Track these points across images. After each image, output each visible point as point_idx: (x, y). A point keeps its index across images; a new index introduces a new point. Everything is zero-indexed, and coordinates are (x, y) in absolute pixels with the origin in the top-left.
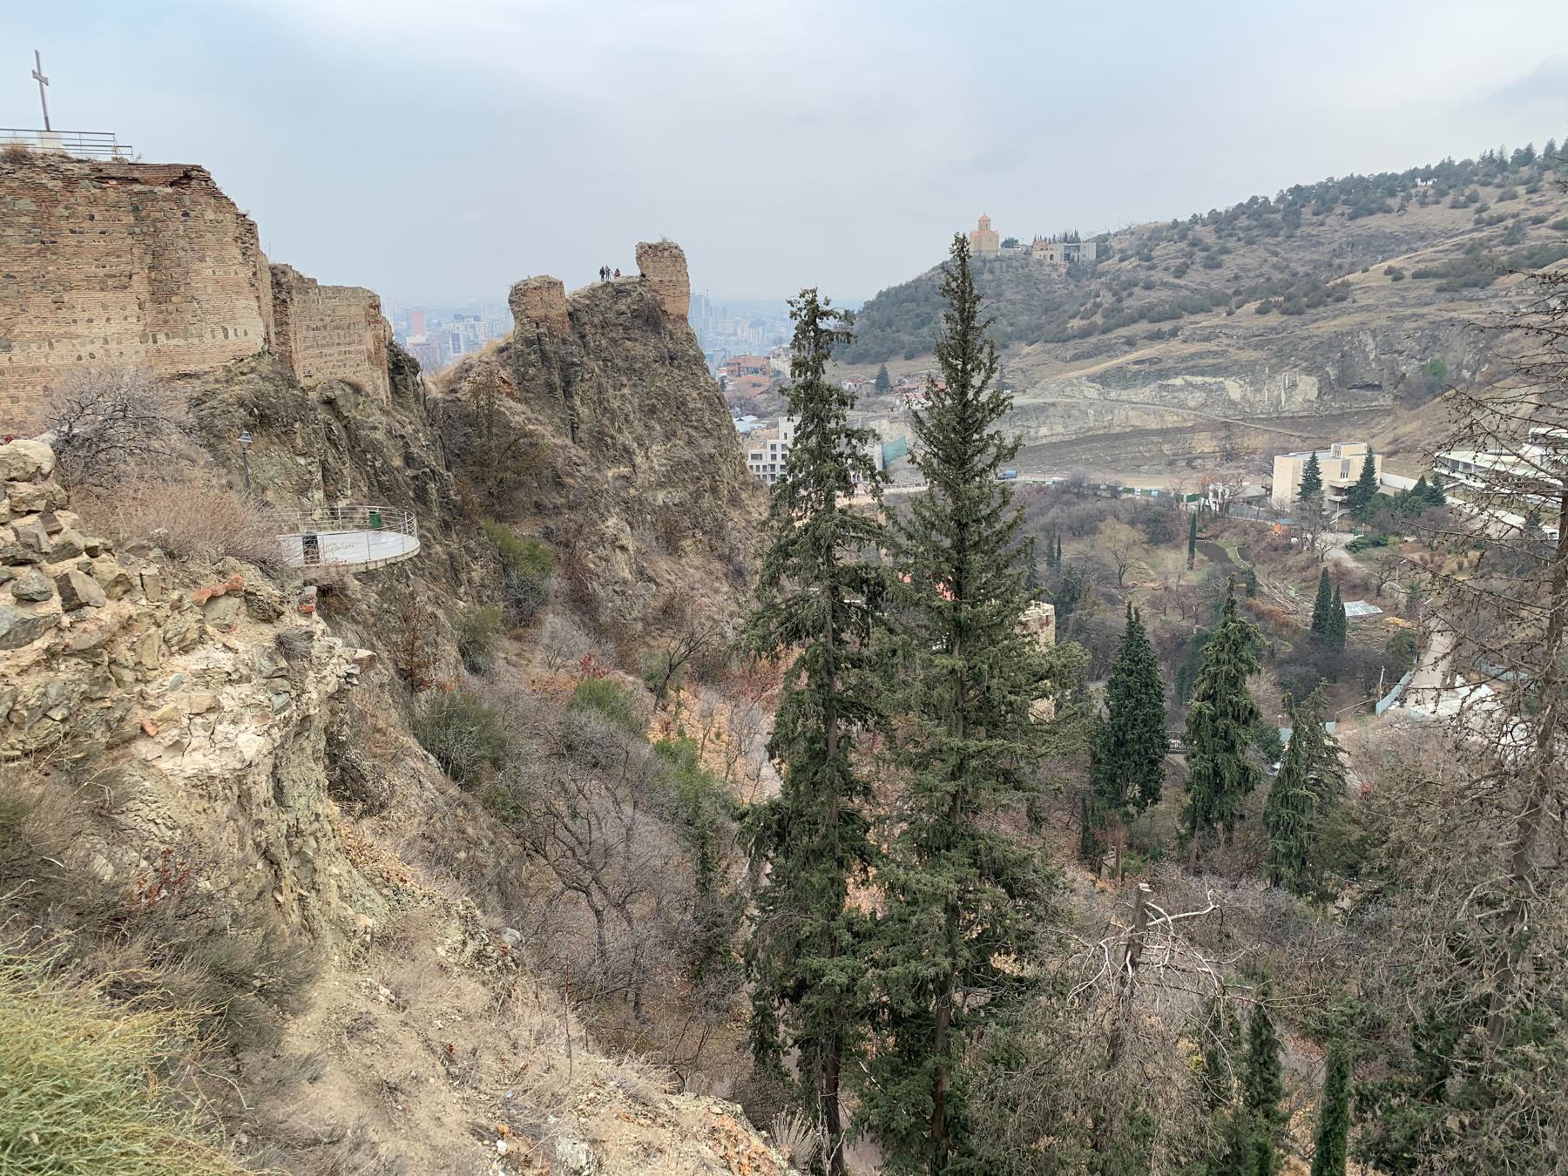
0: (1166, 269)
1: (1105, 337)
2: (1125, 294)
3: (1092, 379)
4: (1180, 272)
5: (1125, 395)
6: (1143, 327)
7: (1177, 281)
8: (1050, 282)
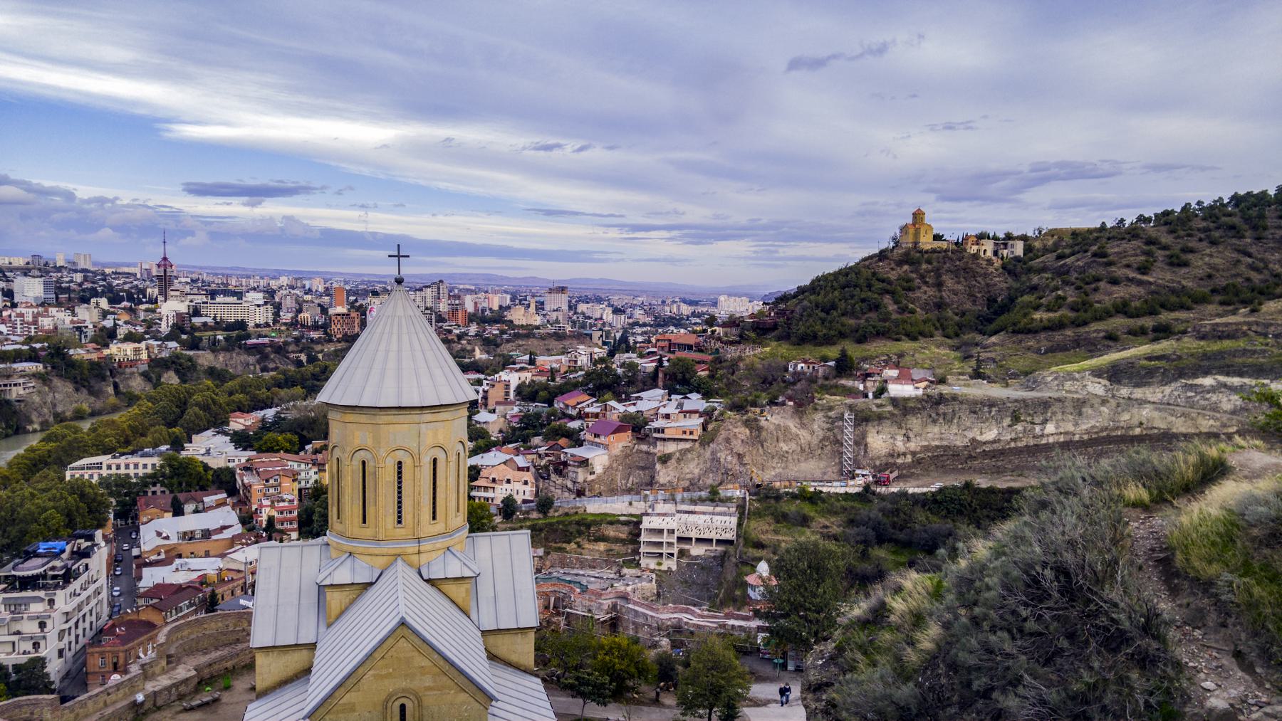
0: (1128, 266)
1: (1082, 330)
2: (1088, 288)
3: (1097, 373)
4: (1144, 269)
5: (1138, 393)
6: (1119, 322)
7: (1145, 278)
8: (986, 275)
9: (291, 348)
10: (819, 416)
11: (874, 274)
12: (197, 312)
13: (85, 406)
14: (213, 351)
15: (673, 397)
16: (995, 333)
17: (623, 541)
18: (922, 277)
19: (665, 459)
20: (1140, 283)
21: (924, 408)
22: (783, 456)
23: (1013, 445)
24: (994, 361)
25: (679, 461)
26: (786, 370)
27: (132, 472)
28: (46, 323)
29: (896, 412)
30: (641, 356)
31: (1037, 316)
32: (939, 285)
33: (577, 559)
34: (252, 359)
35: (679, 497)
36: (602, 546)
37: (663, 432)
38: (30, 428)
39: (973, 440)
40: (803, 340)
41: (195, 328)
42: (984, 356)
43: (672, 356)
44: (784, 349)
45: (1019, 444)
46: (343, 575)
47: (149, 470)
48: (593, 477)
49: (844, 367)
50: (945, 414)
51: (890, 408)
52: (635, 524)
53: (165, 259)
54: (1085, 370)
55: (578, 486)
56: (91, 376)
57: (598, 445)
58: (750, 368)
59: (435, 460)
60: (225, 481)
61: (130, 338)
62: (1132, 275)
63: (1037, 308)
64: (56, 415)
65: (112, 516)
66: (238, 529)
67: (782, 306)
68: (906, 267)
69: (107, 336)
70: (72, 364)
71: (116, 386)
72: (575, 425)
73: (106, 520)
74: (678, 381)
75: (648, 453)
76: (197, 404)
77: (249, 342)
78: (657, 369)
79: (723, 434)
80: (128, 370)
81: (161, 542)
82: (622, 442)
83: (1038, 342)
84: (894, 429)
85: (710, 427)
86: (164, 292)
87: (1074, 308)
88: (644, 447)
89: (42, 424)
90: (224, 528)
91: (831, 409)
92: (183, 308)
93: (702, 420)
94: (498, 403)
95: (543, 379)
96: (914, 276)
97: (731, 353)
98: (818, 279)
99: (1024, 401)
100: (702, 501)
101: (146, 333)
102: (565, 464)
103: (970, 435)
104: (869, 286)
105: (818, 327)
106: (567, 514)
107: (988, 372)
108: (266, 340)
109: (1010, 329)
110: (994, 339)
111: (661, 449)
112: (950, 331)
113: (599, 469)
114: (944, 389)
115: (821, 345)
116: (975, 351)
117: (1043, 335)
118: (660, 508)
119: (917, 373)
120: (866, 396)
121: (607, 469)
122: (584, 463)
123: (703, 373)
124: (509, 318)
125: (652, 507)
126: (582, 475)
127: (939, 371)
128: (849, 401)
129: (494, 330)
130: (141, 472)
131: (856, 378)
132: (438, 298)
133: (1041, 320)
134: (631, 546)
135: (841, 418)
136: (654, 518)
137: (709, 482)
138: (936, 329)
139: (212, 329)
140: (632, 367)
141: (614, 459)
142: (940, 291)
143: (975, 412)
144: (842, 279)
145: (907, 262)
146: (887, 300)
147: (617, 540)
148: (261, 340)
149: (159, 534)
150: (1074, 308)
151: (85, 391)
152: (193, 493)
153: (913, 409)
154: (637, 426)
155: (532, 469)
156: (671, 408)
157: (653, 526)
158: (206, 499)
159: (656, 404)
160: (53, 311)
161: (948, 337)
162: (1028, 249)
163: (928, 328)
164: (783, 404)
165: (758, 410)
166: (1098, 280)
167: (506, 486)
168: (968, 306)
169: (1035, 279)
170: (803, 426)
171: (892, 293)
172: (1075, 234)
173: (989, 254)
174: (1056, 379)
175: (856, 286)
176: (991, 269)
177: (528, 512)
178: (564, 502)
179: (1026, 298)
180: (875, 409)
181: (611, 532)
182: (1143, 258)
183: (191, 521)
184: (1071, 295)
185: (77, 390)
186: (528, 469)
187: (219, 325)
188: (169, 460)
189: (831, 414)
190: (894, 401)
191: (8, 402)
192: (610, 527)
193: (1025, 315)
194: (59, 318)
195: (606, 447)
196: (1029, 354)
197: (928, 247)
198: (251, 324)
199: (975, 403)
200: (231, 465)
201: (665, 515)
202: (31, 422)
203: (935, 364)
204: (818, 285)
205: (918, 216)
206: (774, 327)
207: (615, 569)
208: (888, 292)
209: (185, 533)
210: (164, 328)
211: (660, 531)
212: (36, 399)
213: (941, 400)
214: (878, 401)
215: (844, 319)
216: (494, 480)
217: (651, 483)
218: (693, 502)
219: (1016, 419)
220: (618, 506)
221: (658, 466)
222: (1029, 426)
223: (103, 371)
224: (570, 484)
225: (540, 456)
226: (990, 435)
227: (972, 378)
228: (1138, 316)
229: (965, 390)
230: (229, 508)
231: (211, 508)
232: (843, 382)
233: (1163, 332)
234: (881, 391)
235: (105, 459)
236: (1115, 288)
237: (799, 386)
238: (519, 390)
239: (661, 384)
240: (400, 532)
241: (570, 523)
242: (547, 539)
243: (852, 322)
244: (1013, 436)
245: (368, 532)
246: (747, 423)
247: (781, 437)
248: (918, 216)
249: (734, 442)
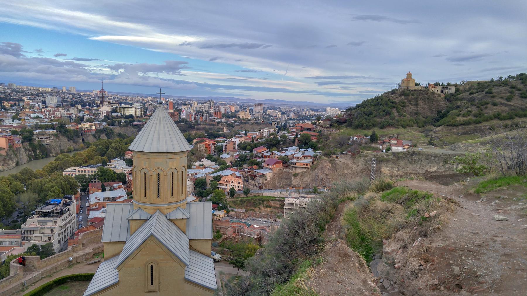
0: (502, 98)
1: (478, 125)
2: (482, 107)
4: (509, 99)
6: (496, 122)
7: (509, 103)
8: (437, 101)
10: (361, 159)
11: (389, 100)
12: (114, 111)
13: (72, 147)
15: (301, 150)
16: (440, 126)
17: (277, 208)
18: (410, 101)
19: (296, 175)
20: (506, 105)
21: (406, 157)
22: (345, 176)
23: (444, 173)
24: (438, 138)
25: (301, 176)
26: (349, 139)
27: (87, 173)
28: (58, 114)
29: (394, 158)
30: (289, 133)
31: (458, 119)
32: (417, 105)
33: (258, 214)
35: (301, 191)
36: (269, 209)
37: (295, 164)
38: (51, 155)
39: (427, 171)
41: (113, 118)
42: (434, 135)
43: (302, 133)
44: (349, 130)
45: (446, 173)
46: (137, 217)
47: (93, 173)
48: (266, 181)
49: (374, 139)
50: (415, 160)
51: (392, 157)
52: (282, 201)
53: (102, 89)
54: (478, 143)
55: (260, 185)
56: (75, 135)
57: (269, 169)
59: (173, 173)
60: (122, 179)
61: (89, 121)
62: (503, 101)
63: (458, 115)
64: (61, 150)
65: (79, 190)
66: (126, 197)
67: (349, 113)
68: (403, 97)
69: (81, 120)
70: (67, 131)
71: (83, 140)
72: (260, 160)
73: (77, 192)
74: (304, 143)
75: (289, 173)
76: (112, 148)
77: (134, 123)
78: (295, 139)
79: (320, 166)
80: (87, 133)
81: (96, 201)
82: (280, 166)
83: (458, 130)
84: (393, 165)
85: (315, 163)
86: (102, 102)
87: (475, 116)
88: (287, 170)
89: (56, 154)
90: (121, 197)
91: (367, 156)
92: (109, 109)
93: (312, 160)
94: (230, 151)
95: (249, 141)
96: (406, 101)
97: (326, 132)
98: (365, 101)
99: (449, 155)
100: (310, 193)
101: (95, 119)
102: (255, 176)
103: (426, 169)
104: (387, 105)
105: (364, 122)
106: (255, 196)
107: (435, 142)
109: (446, 125)
110: (439, 128)
111: (294, 171)
112: (420, 125)
113: (268, 178)
114: (415, 149)
115: (365, 129)
116: (430, 133)
117: (460, 127)
118: (293, 195)
119: (405, 142)
120: (382, 151)
121: (272, 179)
122: (263, 176)
124: (238, 116)
125: (290, 194)
126: (261, 181)
127: (415, 142)
128: (374, 153)
129: (232, 121)
130: (90, 173)
131: (379, 143)
132: (210, 107)
133: (460, 121)
134: (280, 210)
135: (371, 160)
136: (290, 199)
137: (314, 185)
138: (415, 123)
139: (120, 118)
140: (285, 137)
141: (275, 174)
142: (417, 107)
143: (428, 159)
144: (375, 102)
145: (403, 95)
146: (394, 111)
147: (275, 207)
148: (139, 123)
149: (96, 198)
150: (475, 116)
151: (72, 141)
152: (110, 183)
154: (285, 161)
155: (242, 177)
156: (299, 155)
157: (289, 202)
158: (114, 185)
159: (293, 153)
160: (60, 109)
161: (419, 127)
162: (457, 90)
163: (411, 123)
164: (346, 154)
165: (335, 156)
166: (487, 104)
167: (231, 184)
168: (429, 114)
169: (459, 103)
170: (354, 163)
171: (396, 108)
172: (479, 83)
173: (439, 92)
174: (464, 146)
175: (381, 105)
176: (440, 99)
177: (240, 195)
178: (254, 191)
179: (454, 111)
180: (385, 157)
181: (272, 204)
182: (509, 94)
183: (108, 194)
184: (474, 110)
185: (69, 141)
186: (240, 177)
187: (122, 116)
188: (101, 170)
189: (367, 158)
190: (394, 154)
191: (43, 145)
192: (272, 202)
193: (453, 119)
194: (62, 112)
195: (272, 169)
197: (413, 89)
198: (135, 116)
199: (428, 155)
200: (125, 172)
201: (294, 198)
202: (52, 153)
203: (413, 139)
204: (364, 104)
205: (409, 75)
206: (345, 122)
207: (273, 219)
208: (394, 107)
209: (106, 198)
210: (102, 117)
211: (293, 204)
212: (54, 144)
213: (414, 154)
214: (387, 154)
216: (227, 181)
217: (290, 185)
218: (307, 193)
219: (446, 162)
220: (276, 194)
221: (293, 178)
222: (451, 166)
223: (79, 134)
224: (257, 184)
225: (245, 172)
226: (434, 169)
227: (428, 145)
228: (504, 120)
229: (424, 150)
230: (123, 189)
231: (116, 189)
232: (373, 145)
233: (513, 127)
234: (389, 149)
235: (77, 168)
236: (495, 107)
237: (353, 147)
238: (239, 145)
239: (296, 144)
240: (159, 200)
241: (256, 200)
242: (247, 206)
243: (378, 120)
244: (444, 170)
245: (146, 200)
246: (330, 161)
247: (345, 168)
248: (409, 75)
249: (325, 169)
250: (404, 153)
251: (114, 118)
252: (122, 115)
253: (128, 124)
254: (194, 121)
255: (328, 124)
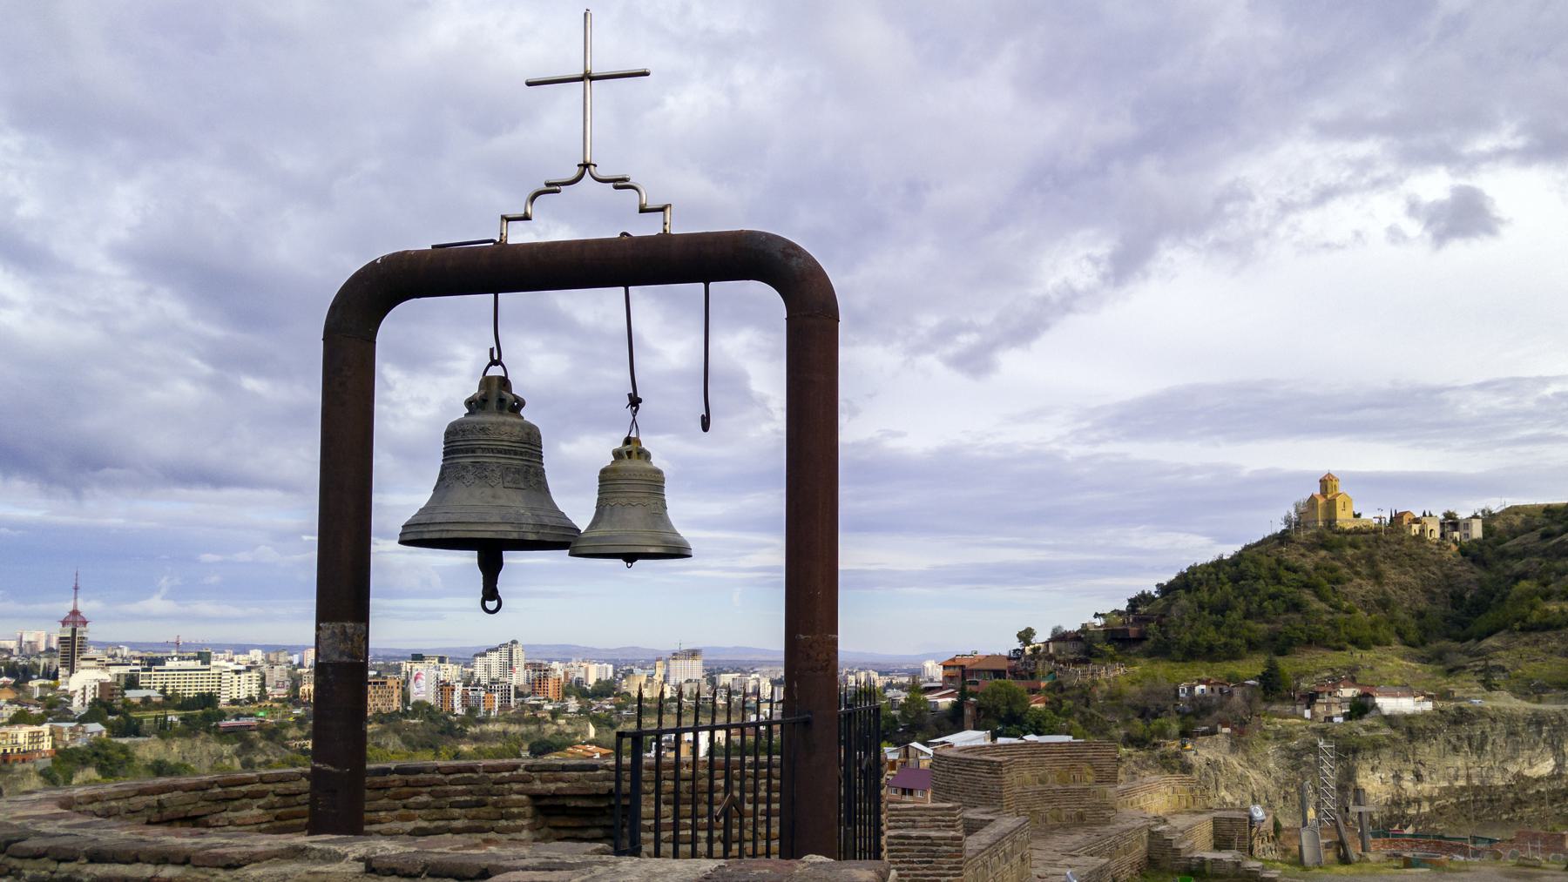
9: (291, 733)
14: (162, 737)
34: (227, 749)
40: (1191, 654)
44: (1161, 669)
58: (1114, 696)
77: (224, 723)
97: (1077, 676)
105: (1211, 634)
108: (253, 721)
123: (1039, 706)
124: (624, 688)
129: (607, 704)
132: (509, 666)
148: (244, 721)
153: (1423, 731)
161: (1412, 645)
176: (1447, 555)
180: (1364, 733)
196: (1556, 658)
206: (1141, 639)
215: (1250, 623)
250: (1424, 715)
251: (134, 707)
252: (167, 698)
253: (190, 728)
254: (459, 710)
255: (1071, 650)
